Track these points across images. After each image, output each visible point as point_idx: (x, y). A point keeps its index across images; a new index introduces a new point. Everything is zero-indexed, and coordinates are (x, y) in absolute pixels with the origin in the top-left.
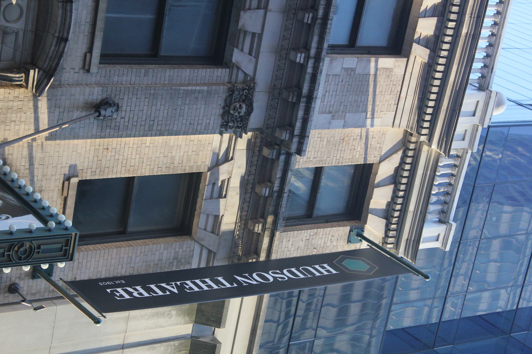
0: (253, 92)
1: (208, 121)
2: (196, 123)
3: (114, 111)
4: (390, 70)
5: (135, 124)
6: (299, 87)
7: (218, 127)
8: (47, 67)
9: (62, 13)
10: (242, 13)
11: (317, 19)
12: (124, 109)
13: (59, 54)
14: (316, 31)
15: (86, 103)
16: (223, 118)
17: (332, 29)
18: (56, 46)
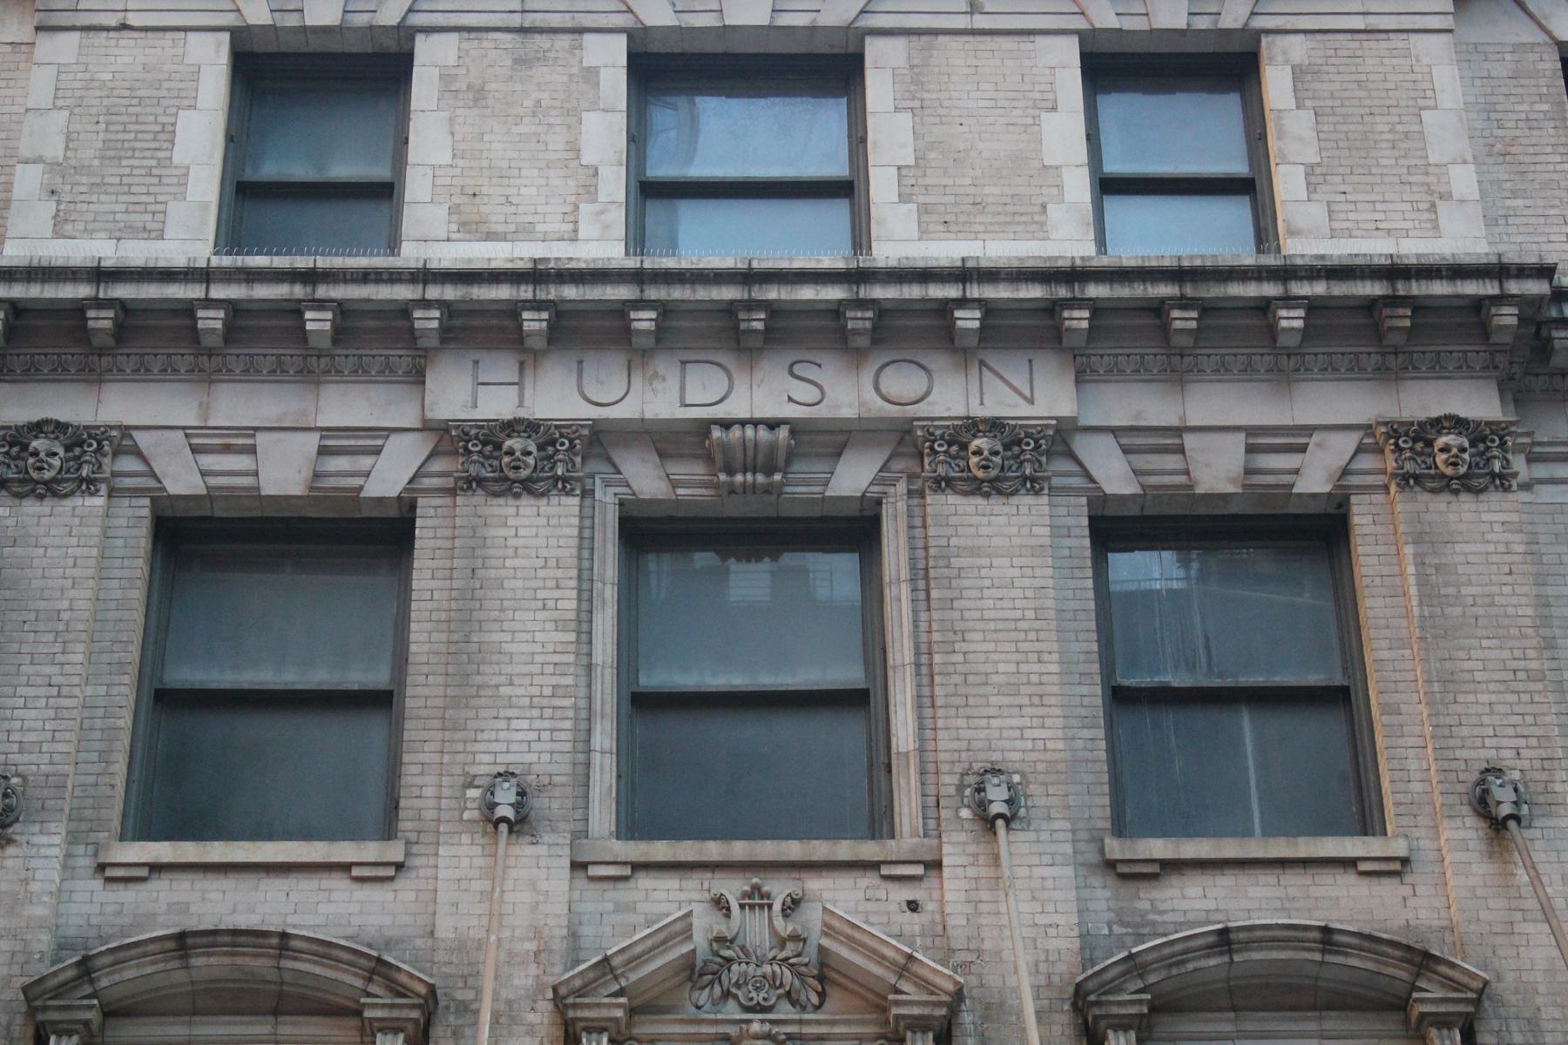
0: (1401, 423)
1: (1497, 528)
2: (1507, 558)
3: (1499, 782)
4: (1298, 73)
5: (1530, 720)
6: (1370, 305)
7: (1510, 496)
8: (1401, 969)
9: (1261, 949)
10: (1199, 490)
11: (1183, 297)
12: (1492, 754)
13: (1366, 944)
14: (1213, 291)
15: (1491, 854)
16: (1484, 490)
17: (1204, 251)
18: (1346, 954)
